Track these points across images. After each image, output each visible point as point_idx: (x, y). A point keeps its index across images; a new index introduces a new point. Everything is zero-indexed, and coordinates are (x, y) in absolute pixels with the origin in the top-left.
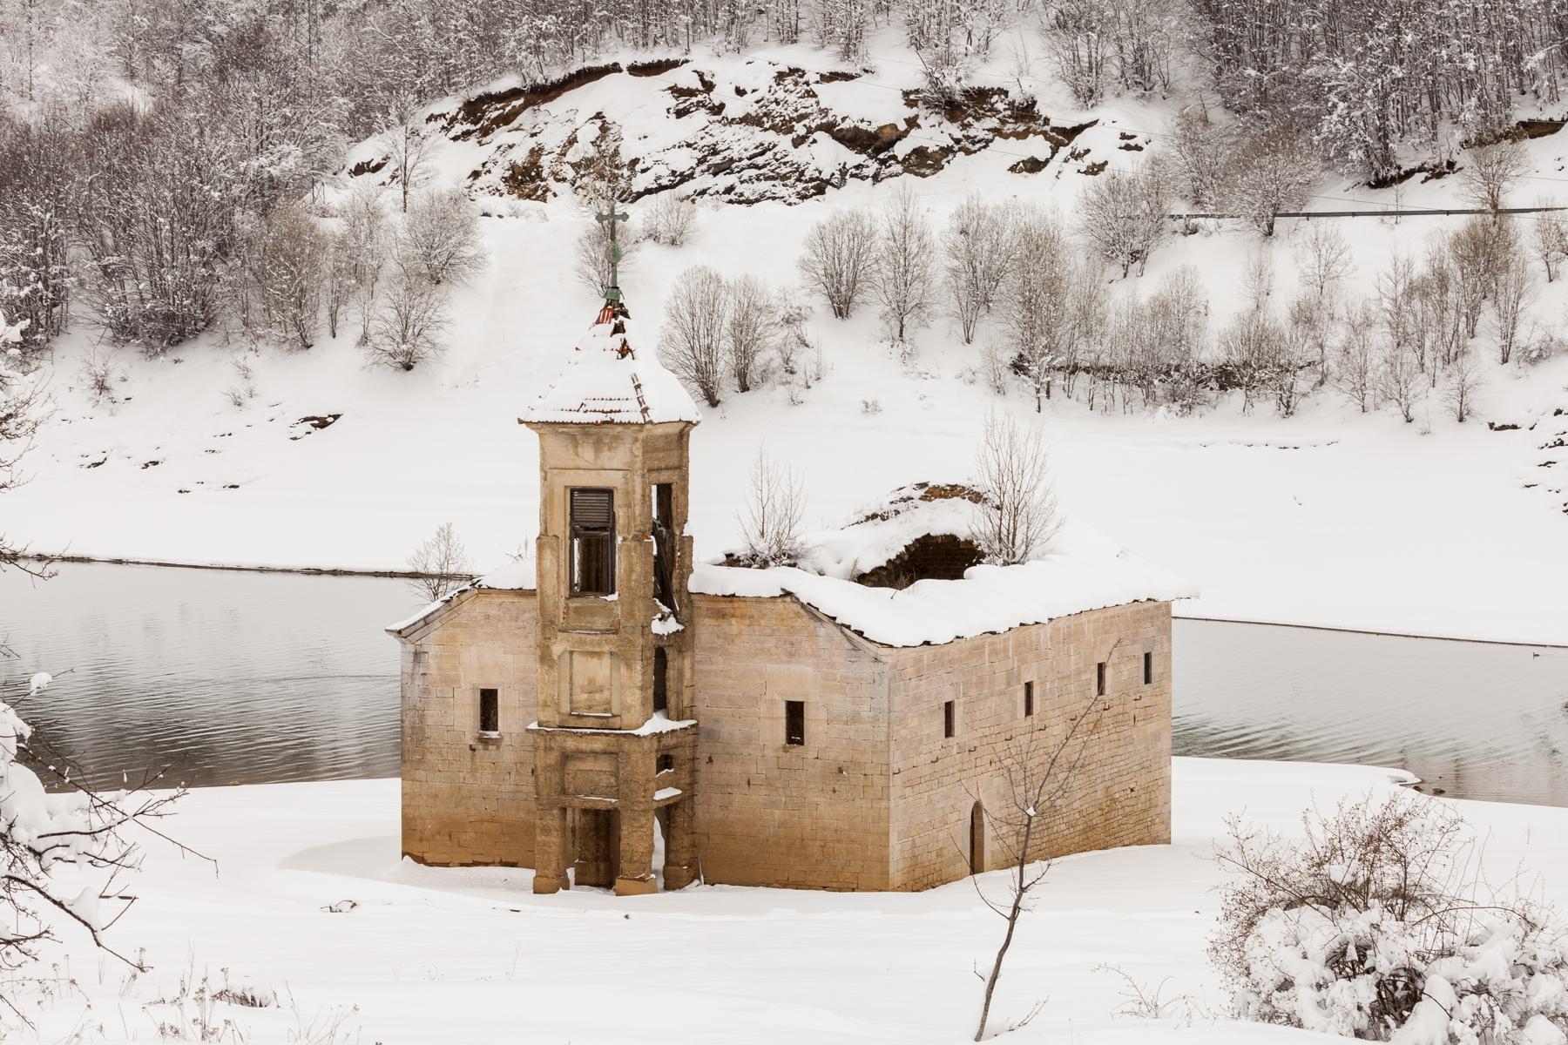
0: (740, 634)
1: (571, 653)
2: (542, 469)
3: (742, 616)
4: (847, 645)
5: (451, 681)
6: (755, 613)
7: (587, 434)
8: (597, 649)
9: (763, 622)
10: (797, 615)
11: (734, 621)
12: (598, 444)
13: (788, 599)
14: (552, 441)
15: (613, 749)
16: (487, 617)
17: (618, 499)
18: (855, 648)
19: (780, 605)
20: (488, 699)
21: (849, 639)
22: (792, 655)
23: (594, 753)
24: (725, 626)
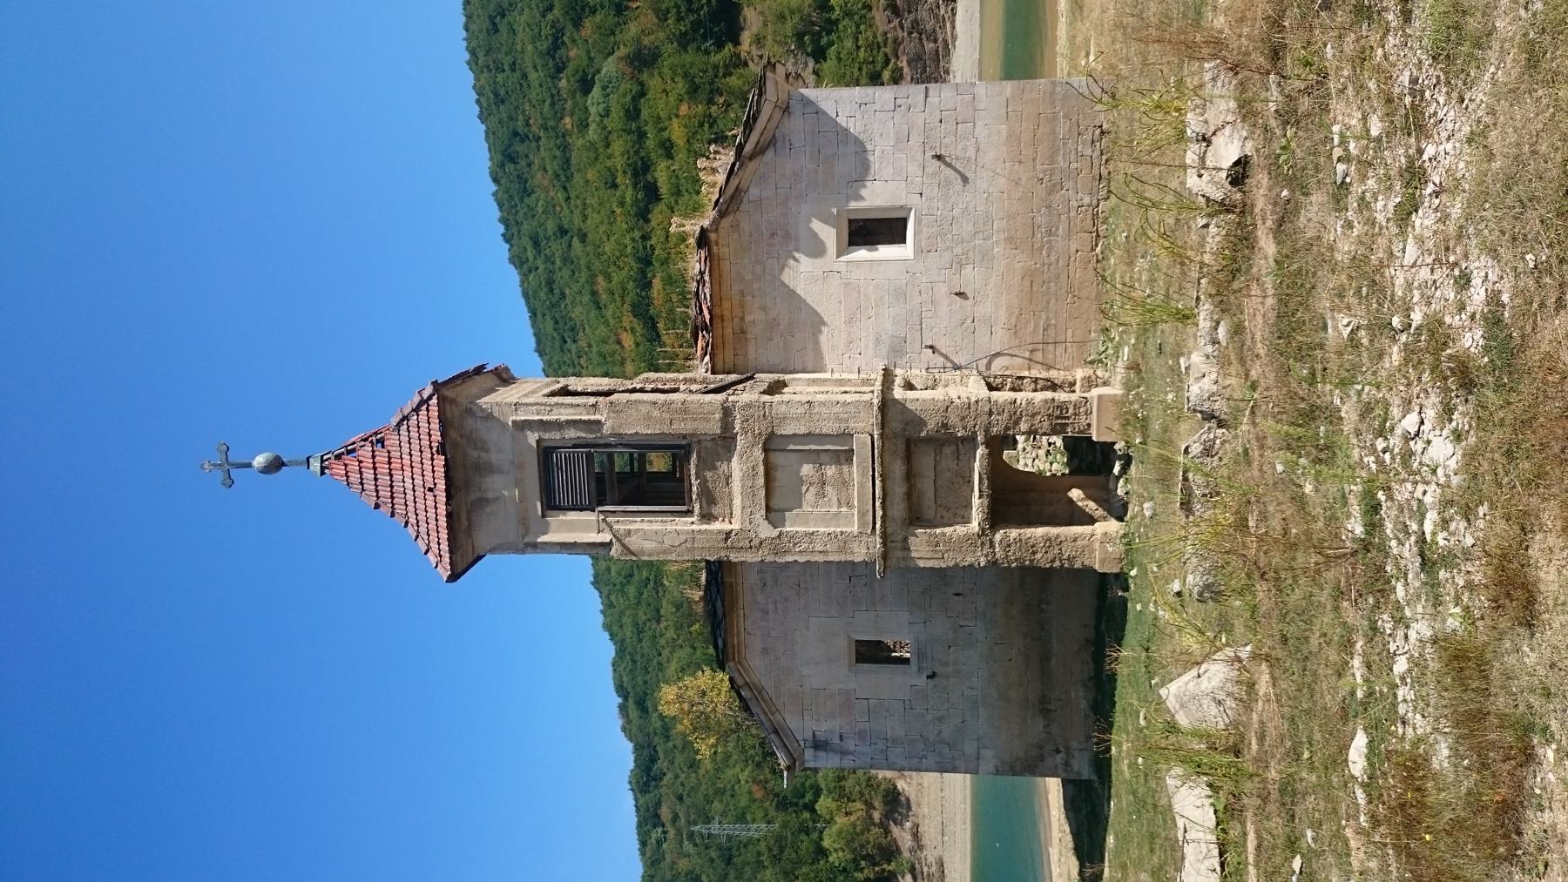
0: (764, 309)
1: (768, 509)
2: (523, 551)
3: (742, 306)
4: (770, 154)
5: (847, 702)
6: (736, 288)
7: (467, 485)
8: (761, 469)
9: (748, 277)
10: (735, 227)
11: (749, 318)
12: (484, 468)
13: (713, 236)
14: (482, 538)
15: (902, 446)
16: (765, 651)
17: (553, 436)
18: (772, 142)
19: (722, 251)
20: (872, 653)
21: (759, 151)
22: (787, 236)
23: (909, 476)
24: (753, 332)
